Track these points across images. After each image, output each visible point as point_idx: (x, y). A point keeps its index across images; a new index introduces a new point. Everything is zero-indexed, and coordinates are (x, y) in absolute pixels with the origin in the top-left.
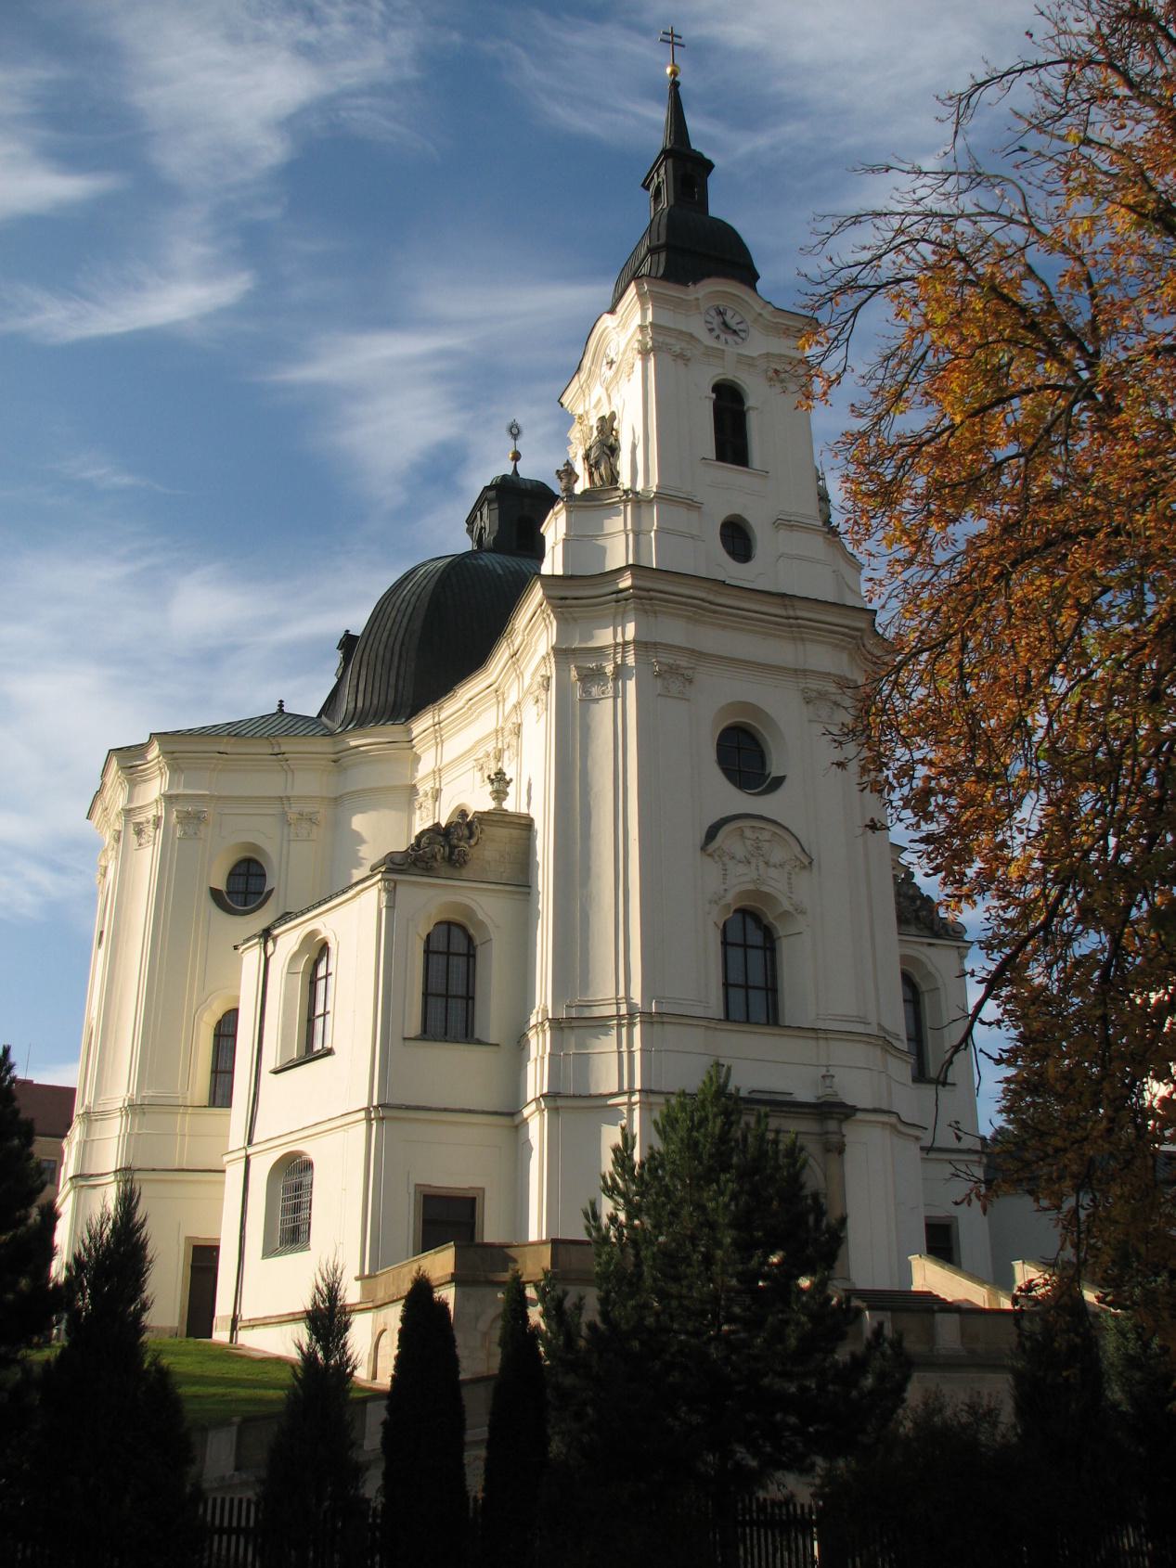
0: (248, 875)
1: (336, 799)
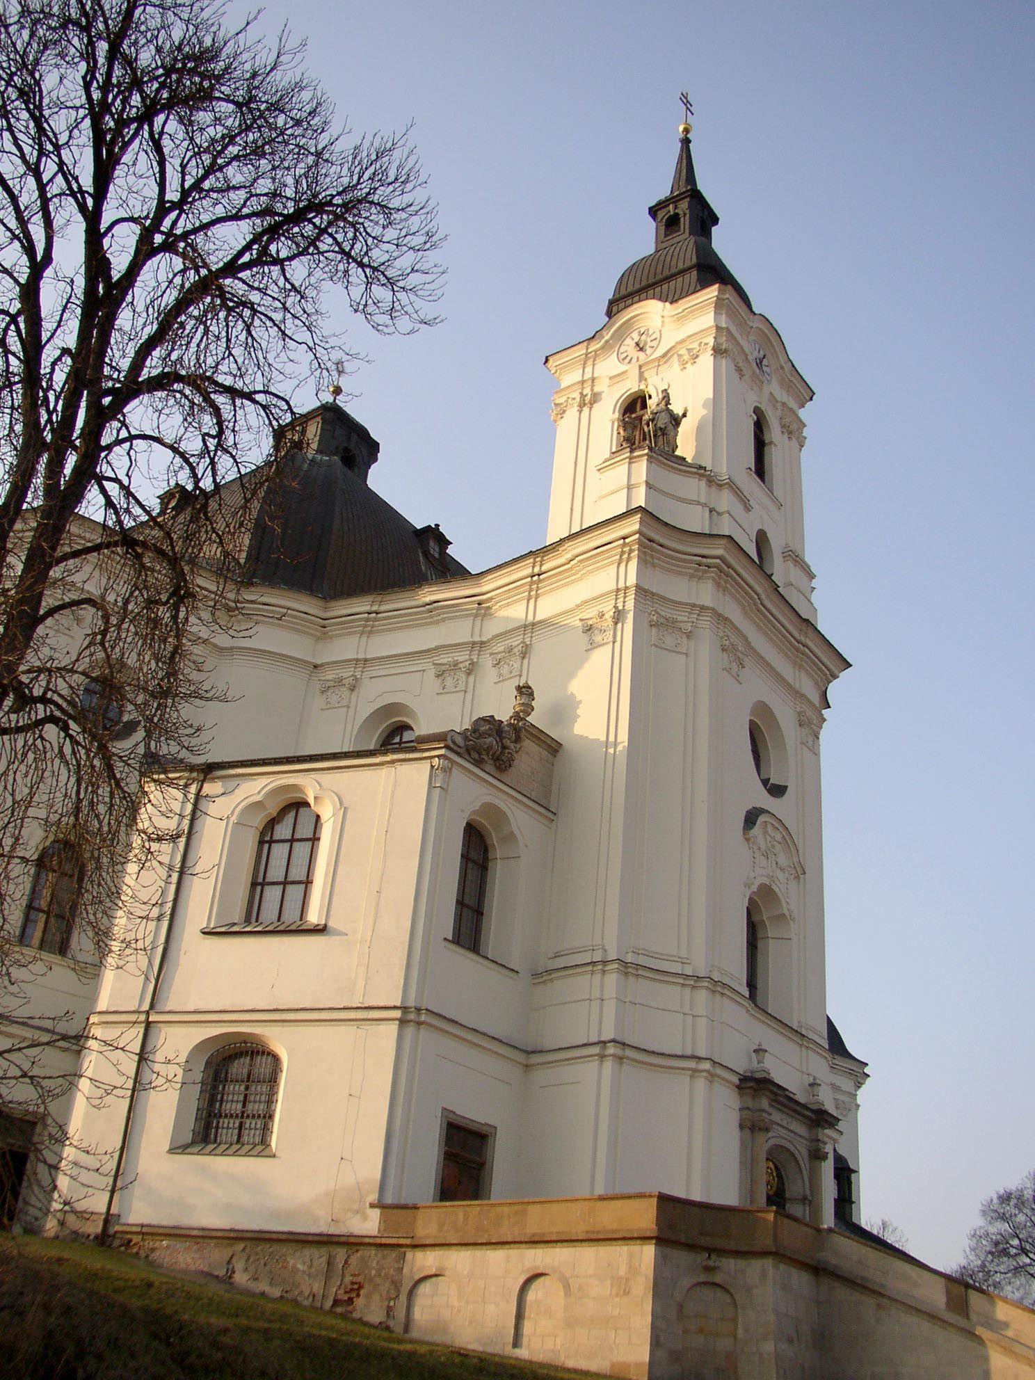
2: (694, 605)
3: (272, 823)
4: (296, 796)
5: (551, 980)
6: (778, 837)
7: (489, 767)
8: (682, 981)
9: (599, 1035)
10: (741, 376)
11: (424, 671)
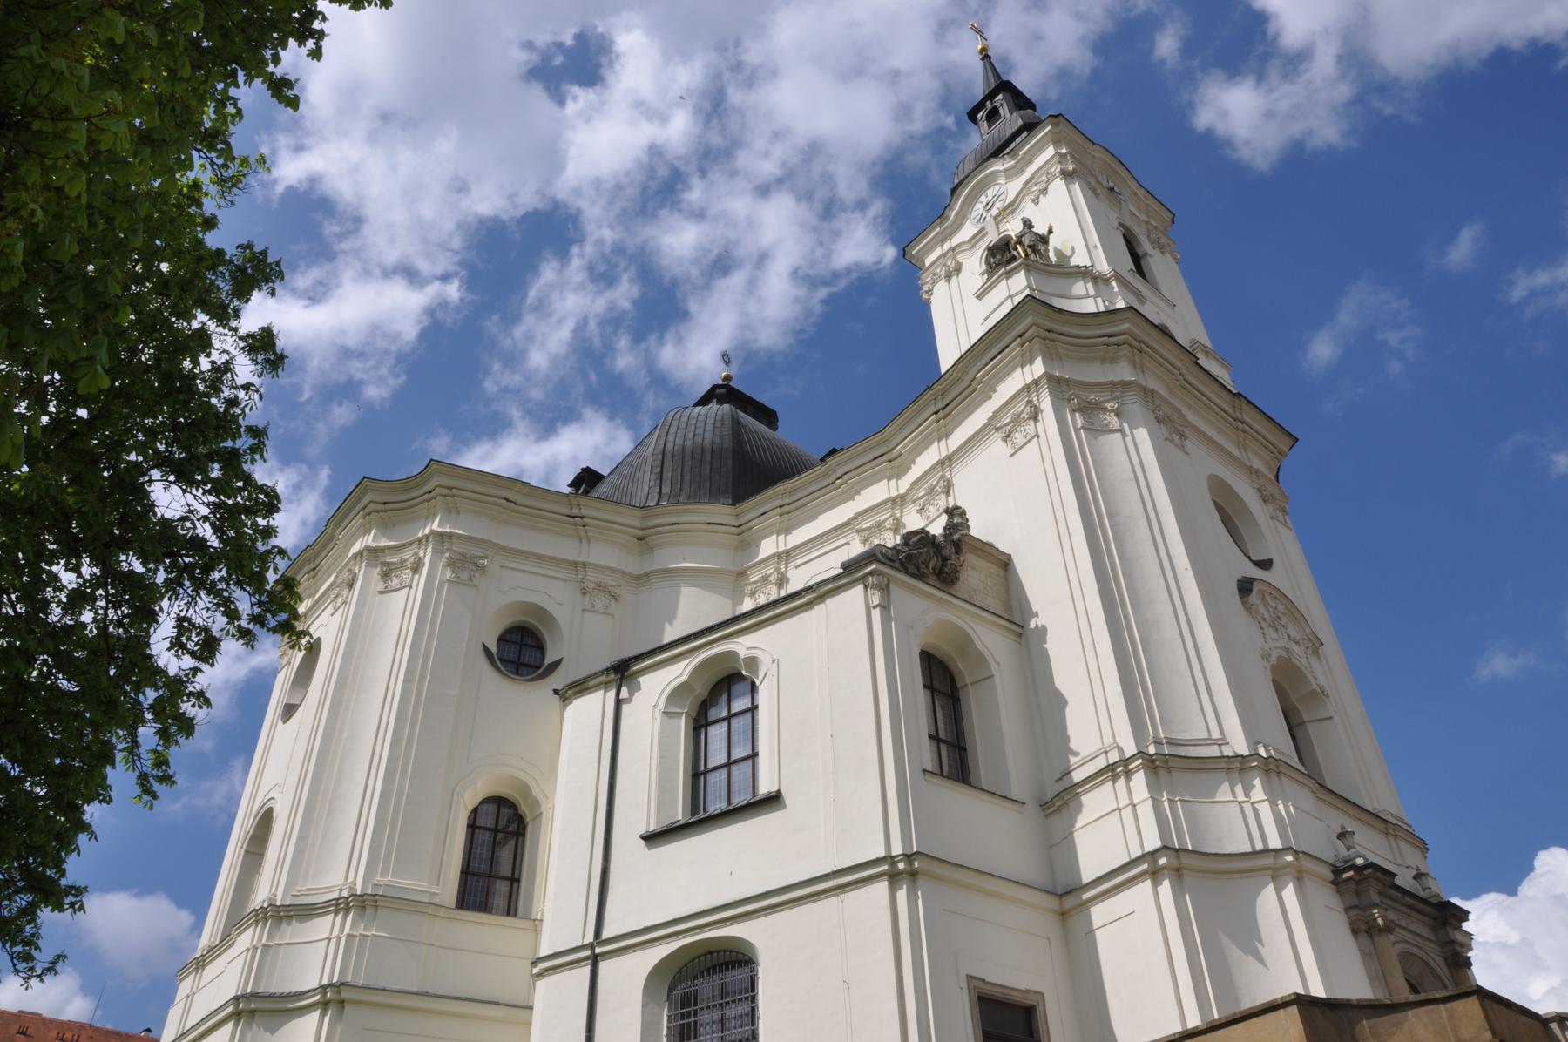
0: (522, 645)
1: (639, 577)
2: (1114, 384)
3: (704, 706)
4: (724, 670)
5: (1066, 804)
6: (1281, 608)
7: (933, 579)
8: (1224, 766)
9: (1142, 847)
10: (1097, 195)
11: (848, 543)
